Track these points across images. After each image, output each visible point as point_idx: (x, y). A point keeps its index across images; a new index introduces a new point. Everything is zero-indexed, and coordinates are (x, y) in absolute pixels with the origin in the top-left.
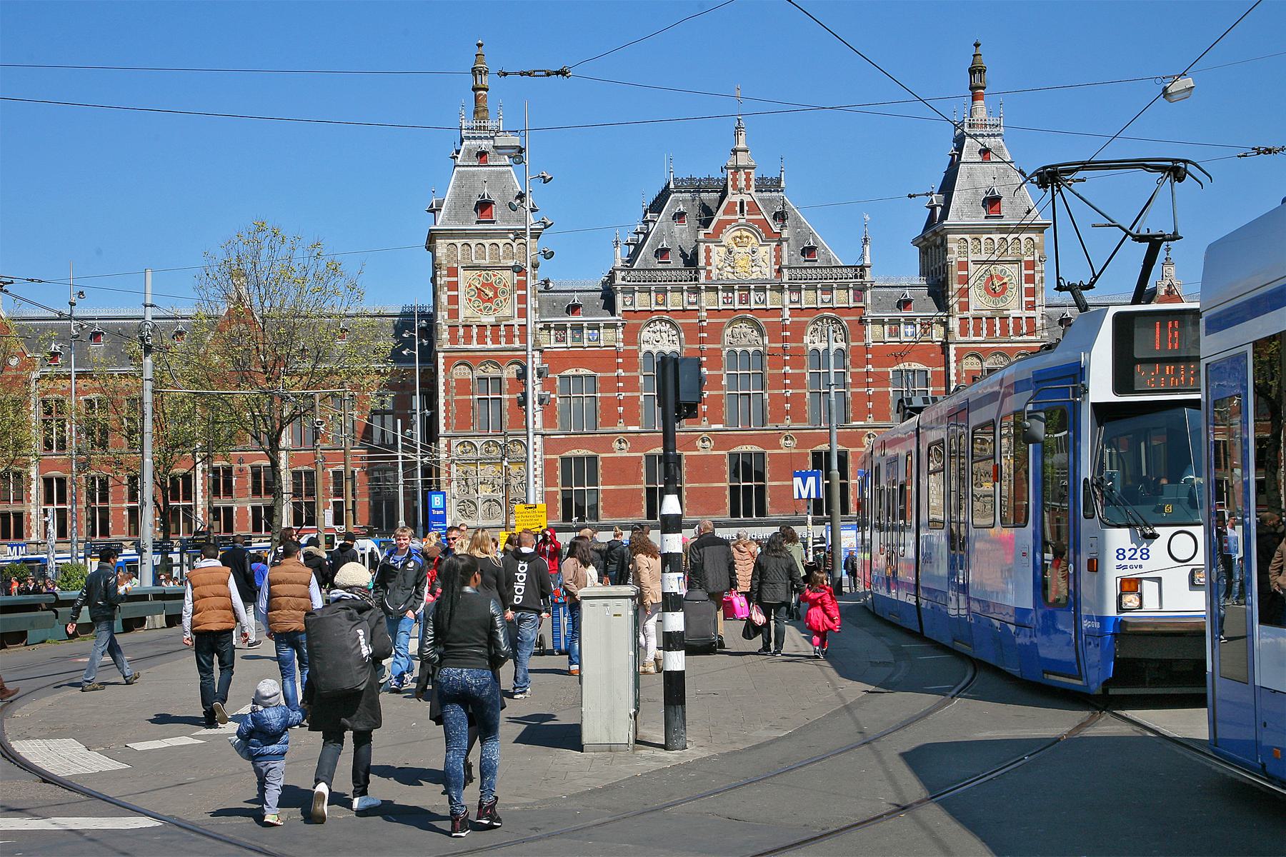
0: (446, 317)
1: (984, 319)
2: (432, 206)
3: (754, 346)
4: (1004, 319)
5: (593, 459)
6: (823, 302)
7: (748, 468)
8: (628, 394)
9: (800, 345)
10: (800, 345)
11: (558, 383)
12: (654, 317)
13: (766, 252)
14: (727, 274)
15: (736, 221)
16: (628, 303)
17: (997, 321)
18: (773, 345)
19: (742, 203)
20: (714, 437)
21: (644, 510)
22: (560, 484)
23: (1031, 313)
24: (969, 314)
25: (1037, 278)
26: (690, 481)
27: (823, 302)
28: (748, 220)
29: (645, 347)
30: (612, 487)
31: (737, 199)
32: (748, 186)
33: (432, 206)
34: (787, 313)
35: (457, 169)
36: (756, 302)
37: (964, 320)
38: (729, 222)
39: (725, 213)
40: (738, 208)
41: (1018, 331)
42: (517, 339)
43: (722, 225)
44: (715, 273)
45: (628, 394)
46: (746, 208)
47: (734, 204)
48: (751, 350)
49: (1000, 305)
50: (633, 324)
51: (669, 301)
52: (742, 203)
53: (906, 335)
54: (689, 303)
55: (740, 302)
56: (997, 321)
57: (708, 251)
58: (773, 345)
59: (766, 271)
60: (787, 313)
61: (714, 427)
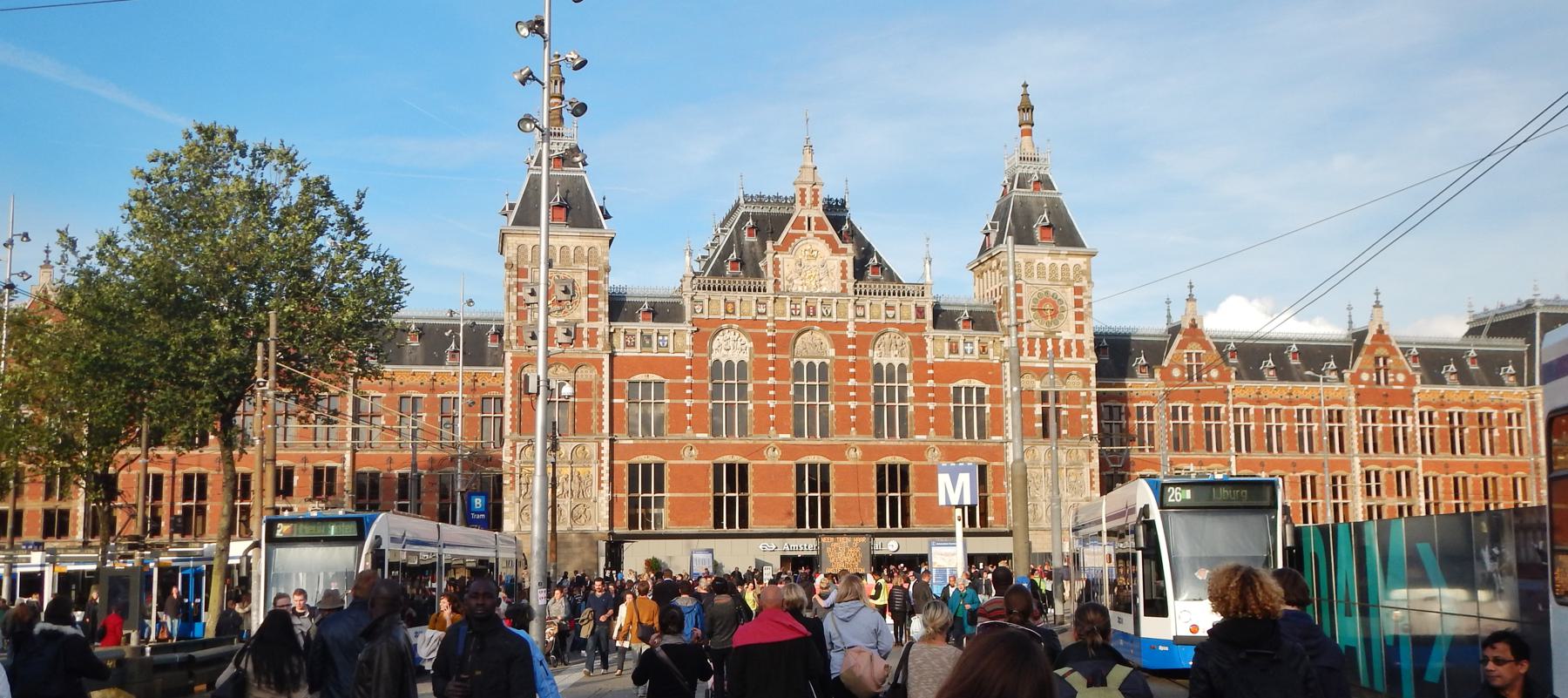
0: (515, 318)
1: (1038, 340)
2: (505, 209)
3: (822, 358)
4: (1056, 341)
5: (660, 467)
6: (887, 317)
7: (818, 478)
8: (698, 401)
9: (866, 358)
10: (866, 358)
11: (627, 388)
12: (724, 326)
13: (835, 262)
14: (798, 287)
15: (805, 235)
16: (698, 311)
17: (1049, 342)
18: (840, 357)
19: (809, 219)
20: (782, 447)
21: (711, 519)
22: (627, 491)
23: (1080, 336)
24: (1024, 335)
25: (1085, 302)
26: (838, 491)
27: (887, 317)
28: (816, 236)
29: (715, 356)
30: (680, 495)
31: (805, 214)
32: (815, 203)
33: (505, 209)
34: (851, 326)
35: (531, 172)
36: (823, 315)
37: (1019, 341)
38: (798, 236)
39: (793, 227)
40: (806, 223)
41: (1068, 352)
42: (585, 343)
43: (791, 238)
44: (784, 285)
45: (698, 401)
46: (813, 224)
47: (799, 220)
48: (817, 362)
49: (1053, 327)
50: (704, 333)
51: (738, 310)
52: (809, 219)
53: (966, 352)
54: (759, 313)
55: (808, 314)
56: (1049, 342)
57: (776, 263)
58: (840, 357)
59: (832, 284)
60: (851, 326)
61: (782, 436)
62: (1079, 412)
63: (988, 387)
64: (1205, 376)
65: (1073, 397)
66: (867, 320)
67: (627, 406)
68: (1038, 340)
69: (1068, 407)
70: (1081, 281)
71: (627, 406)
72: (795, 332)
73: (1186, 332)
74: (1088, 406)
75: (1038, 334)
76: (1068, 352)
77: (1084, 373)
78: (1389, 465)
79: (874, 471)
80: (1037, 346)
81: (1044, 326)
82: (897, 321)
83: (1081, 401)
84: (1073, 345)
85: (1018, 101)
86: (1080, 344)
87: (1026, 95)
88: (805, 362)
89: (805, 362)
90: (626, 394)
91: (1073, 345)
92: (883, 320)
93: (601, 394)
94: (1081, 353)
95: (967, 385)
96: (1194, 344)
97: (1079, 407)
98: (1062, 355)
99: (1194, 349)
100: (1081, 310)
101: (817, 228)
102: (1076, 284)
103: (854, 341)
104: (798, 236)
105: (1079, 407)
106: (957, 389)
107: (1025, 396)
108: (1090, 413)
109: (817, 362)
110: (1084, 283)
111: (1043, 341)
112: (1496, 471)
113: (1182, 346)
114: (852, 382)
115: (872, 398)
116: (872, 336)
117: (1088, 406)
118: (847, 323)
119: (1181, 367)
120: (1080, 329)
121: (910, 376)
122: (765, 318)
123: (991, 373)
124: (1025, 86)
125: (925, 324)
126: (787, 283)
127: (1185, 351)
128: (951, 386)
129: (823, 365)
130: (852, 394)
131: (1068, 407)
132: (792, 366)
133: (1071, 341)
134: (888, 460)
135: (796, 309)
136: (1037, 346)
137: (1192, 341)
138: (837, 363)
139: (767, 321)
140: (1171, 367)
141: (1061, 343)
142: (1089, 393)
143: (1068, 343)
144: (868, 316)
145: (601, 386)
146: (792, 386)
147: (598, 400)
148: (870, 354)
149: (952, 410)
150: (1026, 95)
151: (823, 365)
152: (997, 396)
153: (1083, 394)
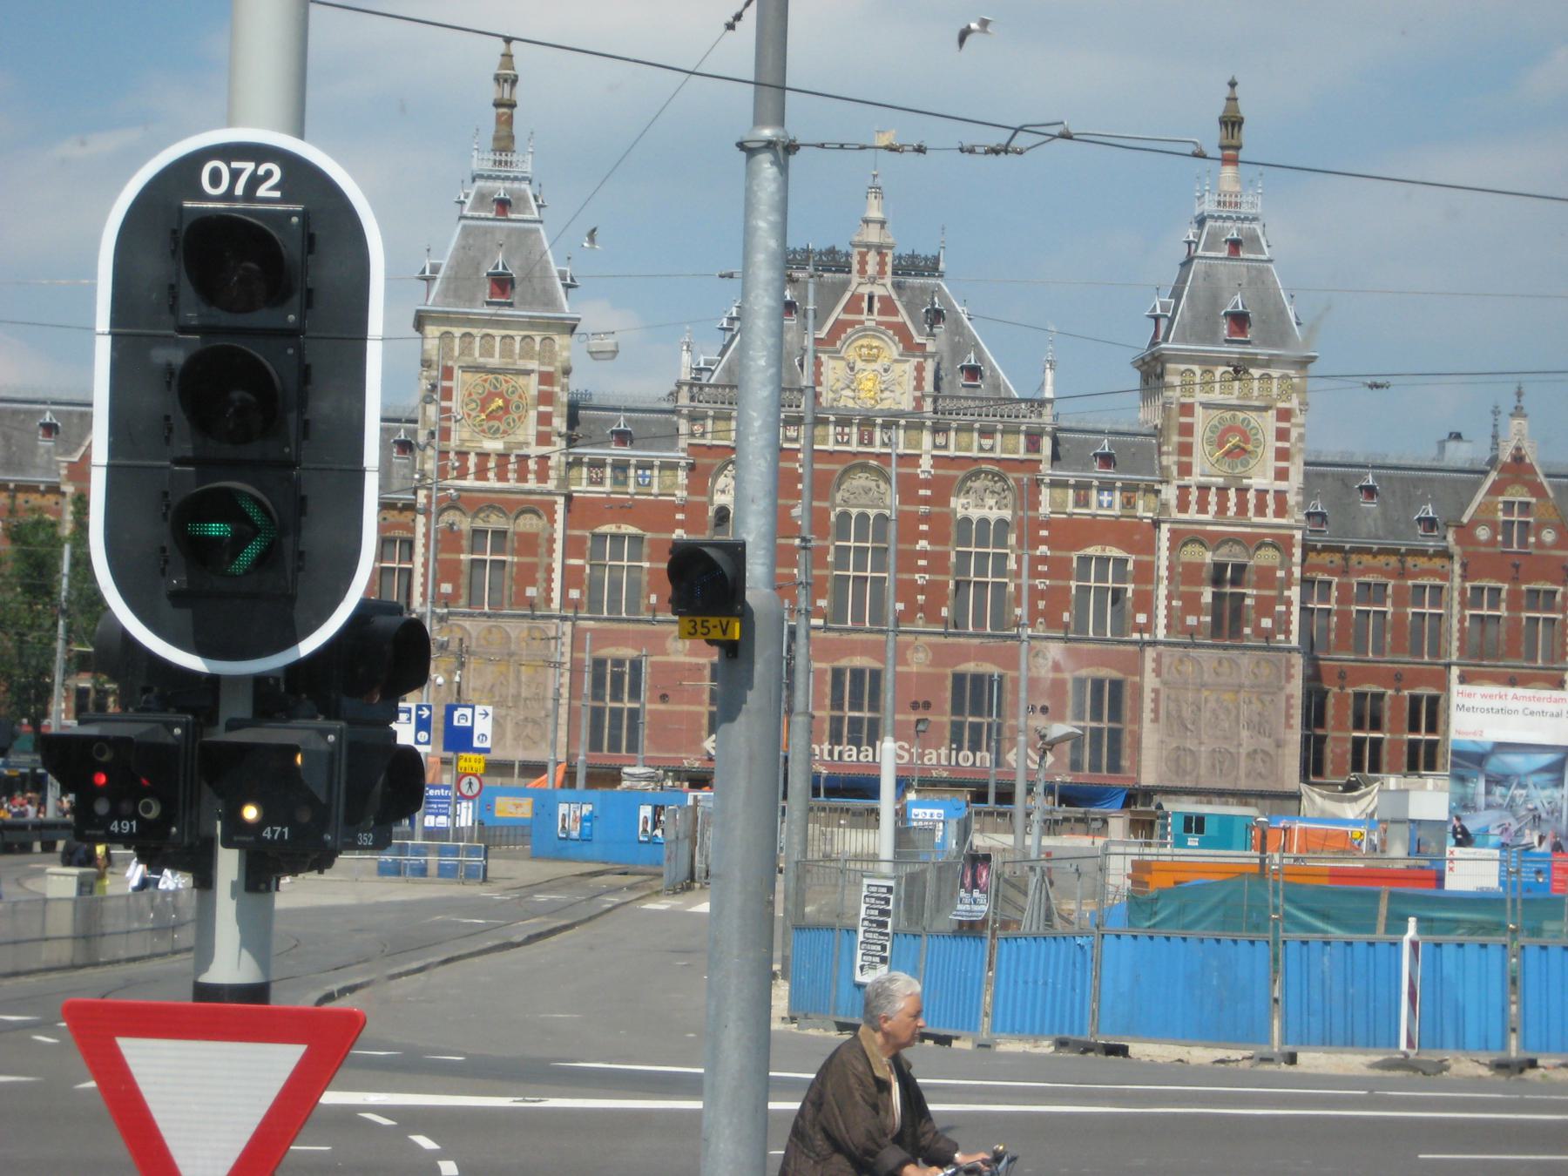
1: (1213, 490)
3: (879, 507)
9: (945, 510)
11: (589, 544)
15: (862, 322)
17: (1232, 493)
18: (907, 508)
24: (1194, 479)
27: (981, 449)
31: (865, 290)
34: (926, 463)
38: (852, 324)
39: (846, 310)
40: (865, 305)
41: (1261, 509)
46: (877, 305)
47: (856, 299)
48: (872, 513)
49: (1239, 470)
53: (1100, 505)
56: (1232, 493)
58: (907, 508)
60: (926, 463)
62: (1273, 601)
63: (1132, 558)
64: (1532, 539)
65: (1265, 577)
66: (951, 452)
67: (588, 570)
68: (1213, 490)
69: (1255, 592)
70: (1289, 399)
71: (588, 570)
72: (839, 468)
73: (1505, 468)
74: (1286, 593)
75: (1213, 479)
76: (1261, 509)
77: (1282, 544)
78: (1398, 679)
79: (949, 683)
80: (1212, 498)
81: (1225, 468)
82: (998, 454)
83: (1277, 584)
84: (1270, 499)
85: (1219, 108)
86: (1280, 496)
87: (1232, 99)
88: (854, 512)
89: (854, 512)
90: (588, 553)
91: (1270, 499)
92: (975, 453)
93: (551, 551)
94: (1281, 510)
95: (1098, 554)
96: (1517, 487)
97: (1272, 593)
98: (1251, 513)
99: (1518, 495)
100: (1286, 445)
101: (881, 313)
102: (1281, 405)
103: (926, 484)
104: (852, 324)
105: (1272, 593)
106: (1085, 561)
107: (1185, 575)
108: (1288, 603)
109: (872, 513)
110: (1294, 403)
111: (1222, 491)
112: (1379, 684)
113: (1496, 489)
114: (923, 544)
115: (952, 570)
116: (955, 477)
117: (1286, 593)
118: (919, 456)
119: (1493, 525)
120: (1282, 474)
121: (1012, 539)
122: (796, 446)
123: (1139, 537)
124: (1233, 84)
125: (1040, 461)
126: (831, 395)
127: (1501, 499)
128: (1075, 555)
129: (882, 518)
130: (922, 562)
131: (1255, 592)
132: (833, 518)
133: (1267, 491)
134: (970, 667)
135: (842, 434)
136: (1212, 498)
137: (1513, 482)
138: (902, 515)
139: (798, 450)
140: (1474, 523)
141: (1251, 495)
142: (1289, 573)
143: (1262, 494)
144: (952, 446)
145: (552, 540)
146: (832, 548)
147: (546, 560)
148: (953, 505)
149: (1074, 591)
150: (1232, 99)
151: (882, 518)
152: (1146, 573)
153: (1280, 574)
